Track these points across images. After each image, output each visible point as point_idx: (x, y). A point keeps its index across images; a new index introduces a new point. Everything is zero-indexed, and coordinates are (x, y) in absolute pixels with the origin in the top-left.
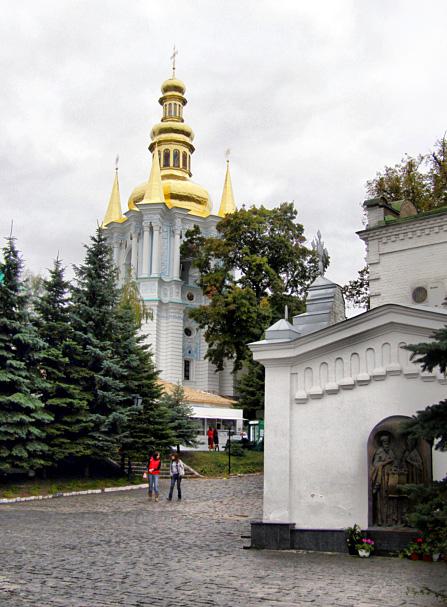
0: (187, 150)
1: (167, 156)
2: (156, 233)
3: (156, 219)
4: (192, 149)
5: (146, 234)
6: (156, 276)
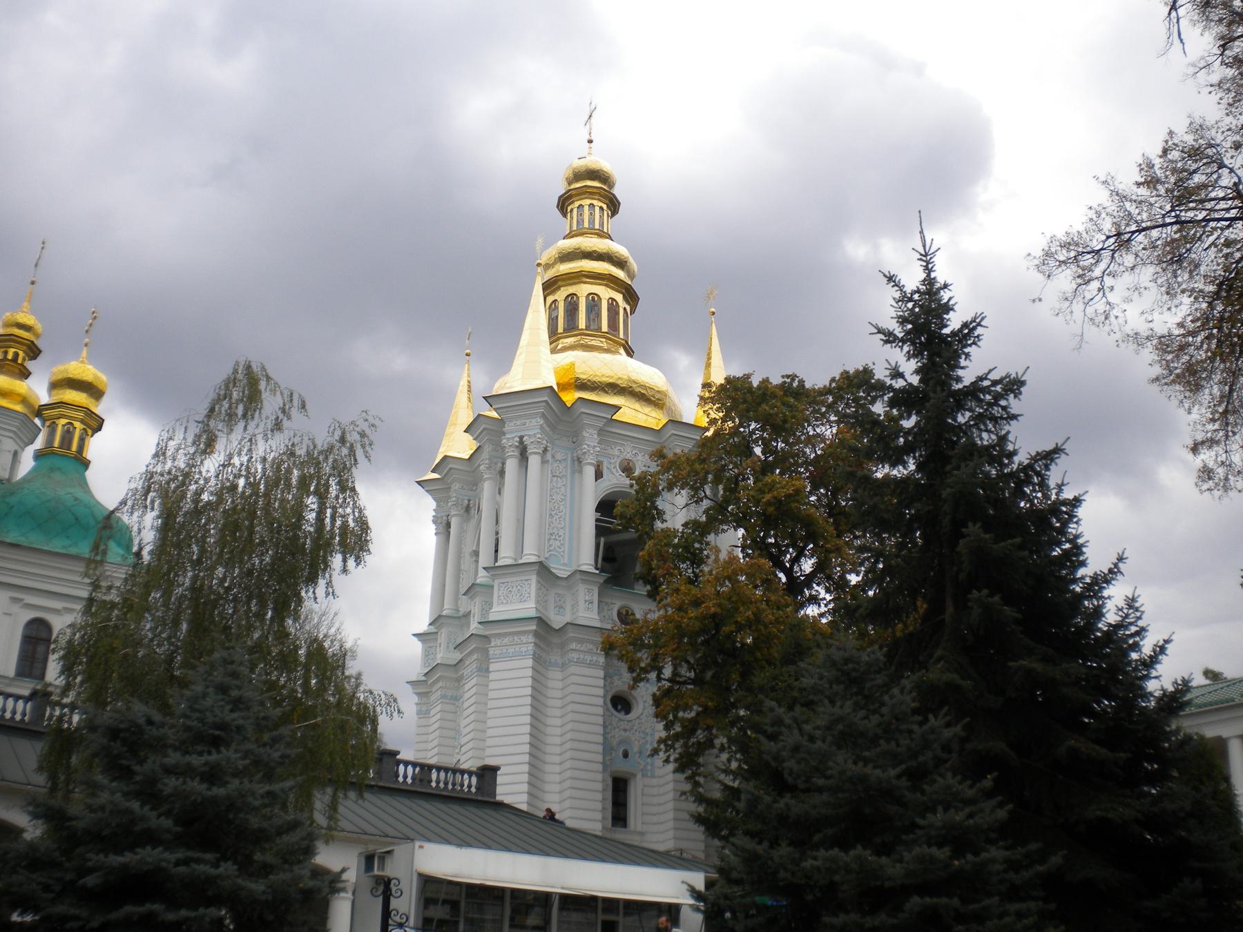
0: (619, 297)
1: (572, 309)
2: (534, 461)
3: (532, 428)
4: (631, 296)
5: (511, 465)
6: (533, 559)
